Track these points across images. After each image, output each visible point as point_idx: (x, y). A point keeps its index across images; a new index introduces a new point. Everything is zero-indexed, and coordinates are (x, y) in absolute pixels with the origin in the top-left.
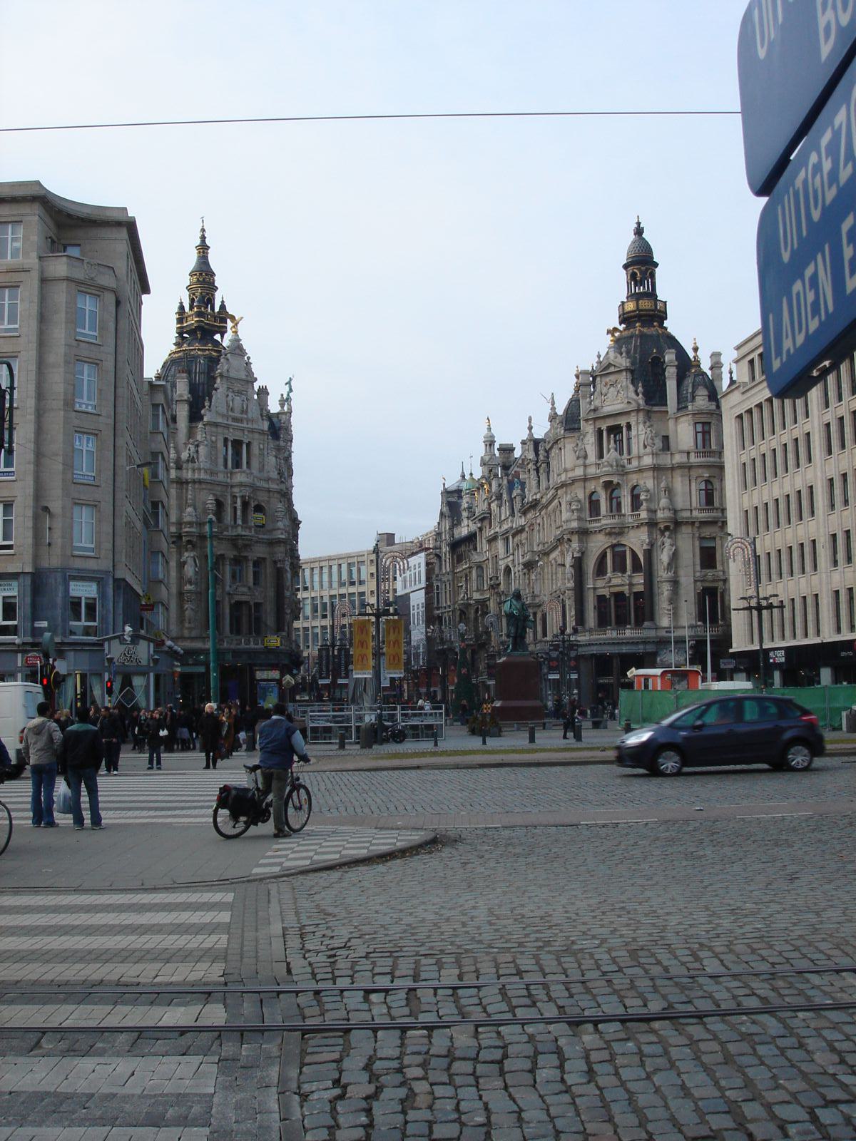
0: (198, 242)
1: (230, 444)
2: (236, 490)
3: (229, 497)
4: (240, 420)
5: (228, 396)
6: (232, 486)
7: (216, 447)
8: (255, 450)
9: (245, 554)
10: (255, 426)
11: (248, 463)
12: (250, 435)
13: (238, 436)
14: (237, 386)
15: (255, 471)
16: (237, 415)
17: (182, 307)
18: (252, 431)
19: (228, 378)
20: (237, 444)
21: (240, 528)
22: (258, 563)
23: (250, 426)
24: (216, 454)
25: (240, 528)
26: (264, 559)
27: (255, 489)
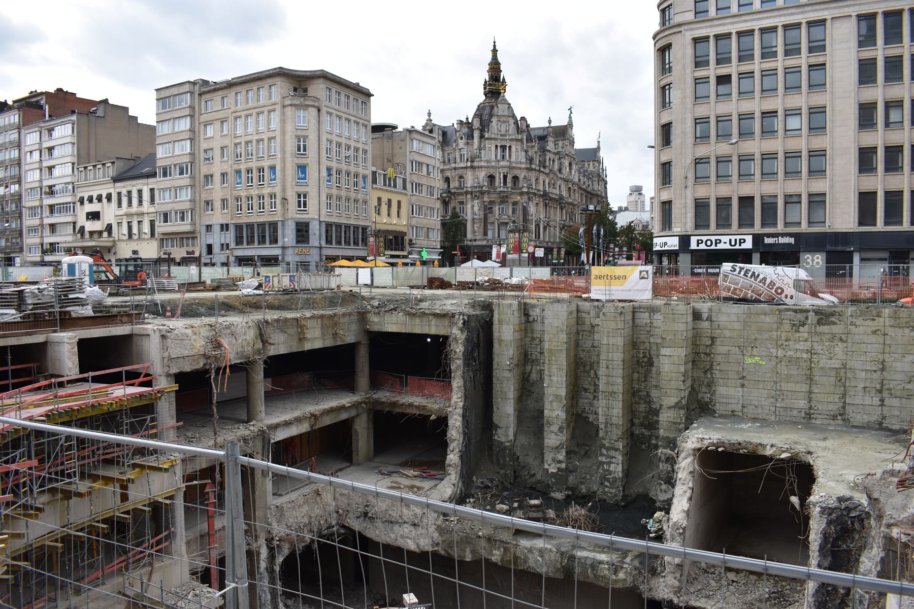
4: (505, 135)
8: (513, 149)
11: (510, 156)
13: (503, 143)
14: (503, 119)
15: (513, 158)
16: (503, 132)
17: (486, 82)
18: (512, 140)
20: (503, 148)
22: (515, 203)
27: (511, 168)
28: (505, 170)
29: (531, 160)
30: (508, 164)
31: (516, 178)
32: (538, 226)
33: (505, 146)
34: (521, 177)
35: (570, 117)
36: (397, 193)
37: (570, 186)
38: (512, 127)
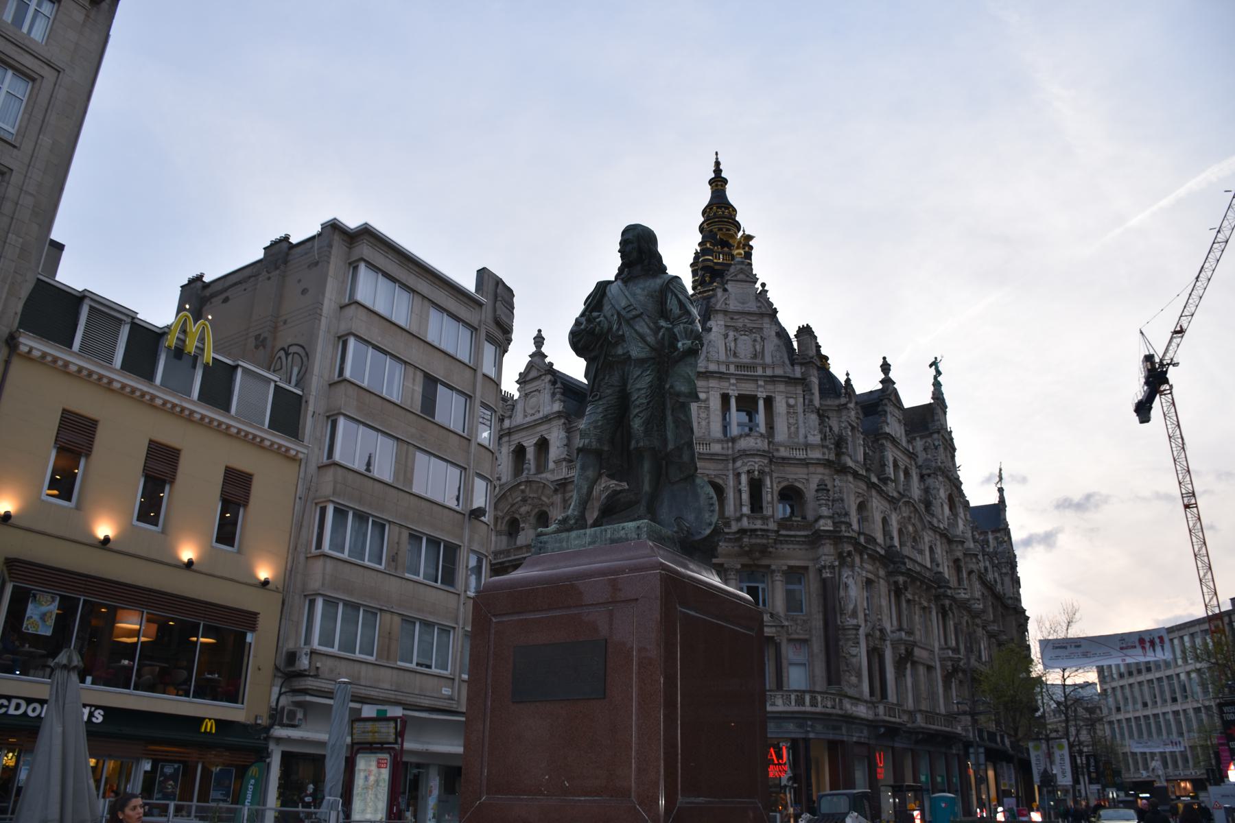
0: (713, 175)
1: (733, 402)
2: (739, 464)
3: (731, 476)
5: (726, 336)
6: (734, 461)
7: (707, 408)
8: (780, 406)
9: (765, 562)
10: (779, 372)
12: (770, 387)
13: (748, 388)
16: (747, 361)
18: (773, 379)
19: (725, 312)
21: (745, 520)
22: (795, 574)
23: (769, 372)
24: (708, 417)
25: (745, 520)
26: (806, 568)
28: (756, 464)
29: (840, 443)
30: (762, 445)
31: (790, 495)
32: (875, 653)
33: (753, 399)
34: (810, 490)
35: (937, 385)
36: (225, 431)
37: (959, 554)
38: (772, 344)
